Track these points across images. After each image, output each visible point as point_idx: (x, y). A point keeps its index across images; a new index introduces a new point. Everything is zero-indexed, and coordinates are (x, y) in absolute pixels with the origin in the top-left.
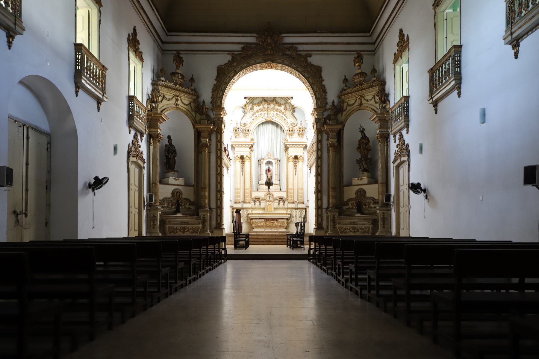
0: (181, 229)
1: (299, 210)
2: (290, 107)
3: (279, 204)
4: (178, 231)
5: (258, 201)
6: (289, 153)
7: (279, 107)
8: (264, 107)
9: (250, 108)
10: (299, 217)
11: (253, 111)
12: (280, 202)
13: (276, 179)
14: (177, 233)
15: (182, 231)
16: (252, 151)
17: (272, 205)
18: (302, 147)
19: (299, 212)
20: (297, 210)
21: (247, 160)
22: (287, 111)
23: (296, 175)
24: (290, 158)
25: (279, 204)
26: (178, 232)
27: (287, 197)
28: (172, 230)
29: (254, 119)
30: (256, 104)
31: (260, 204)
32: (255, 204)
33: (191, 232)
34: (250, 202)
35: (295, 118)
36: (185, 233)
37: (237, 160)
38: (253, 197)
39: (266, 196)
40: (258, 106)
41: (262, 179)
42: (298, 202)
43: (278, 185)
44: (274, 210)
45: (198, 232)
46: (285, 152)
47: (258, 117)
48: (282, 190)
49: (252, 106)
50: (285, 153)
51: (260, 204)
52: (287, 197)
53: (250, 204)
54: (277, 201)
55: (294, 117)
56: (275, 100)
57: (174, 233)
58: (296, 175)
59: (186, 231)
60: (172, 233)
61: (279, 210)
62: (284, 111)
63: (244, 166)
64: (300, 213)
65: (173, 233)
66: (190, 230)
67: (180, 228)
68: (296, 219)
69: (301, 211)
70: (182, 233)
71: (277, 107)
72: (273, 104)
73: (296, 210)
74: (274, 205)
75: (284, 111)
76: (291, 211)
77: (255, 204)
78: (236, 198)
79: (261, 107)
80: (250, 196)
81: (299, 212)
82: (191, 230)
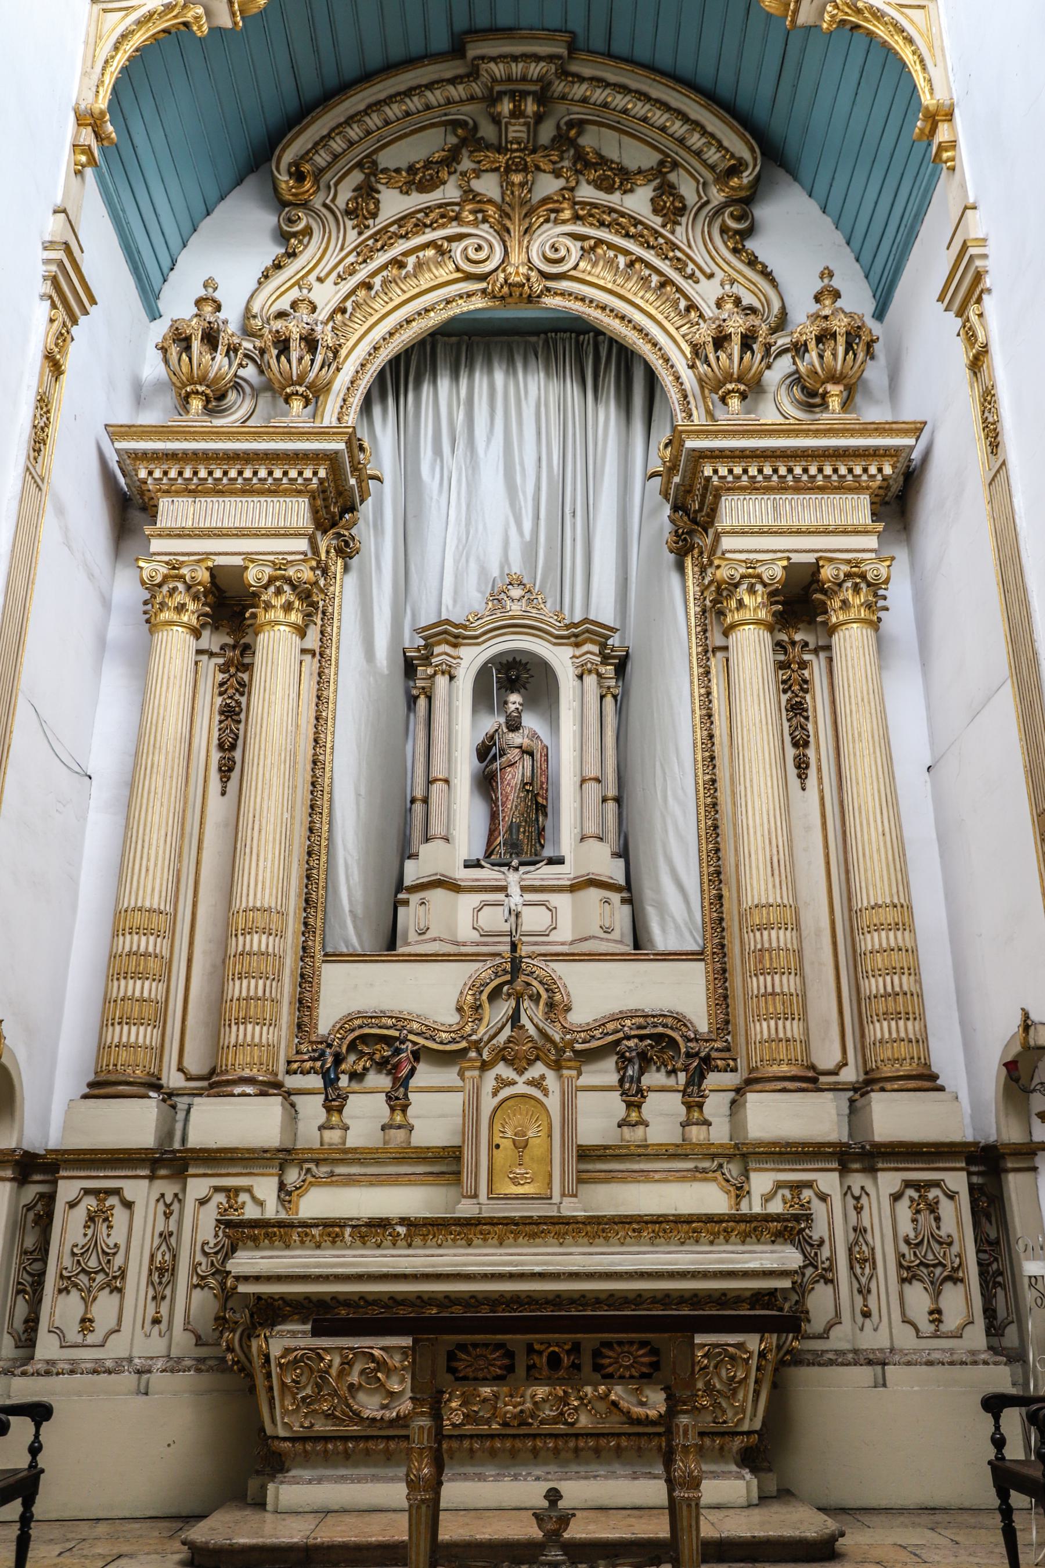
1: (889, 1181)
2: (714, 190)
3: (634, 1100)
5: (382, 1065)
6: (727, 543)
7: (610, 190)
8: (470, 195)
9: (343, 206)
10: (908, 1275)
11: (371, 222)
12: (646, 1080)
13: (591, 828)
16: (346, 550)
17: (553, 1102)
18: (857, 489)
19: (896, 1197)
20: (871, 1170)
21: (271, 615)
22: (684, 220)
23: (802, 776)
24: (742, 592)
25: (634, 1100)
27: (724, 1024)
29: (377, 281)
30: (398, 171)
31: (398, 1102)
32: (335, 1103)
34: (292, 1082)
35: (767, 274)
37: (165, 616)
38: (326, 1020)
39: (477, 1008)
40: (423, 188)
41: (436, 829)
42: (850, 1075)
43: (616, 897)
44: (580, 1181)
46: (681, 568)
47: (419, 265)
48: (662, 939)
49: (367, 192)
50: (675, 578)
51: (398, 1102)
52: (724, 1024)
53: (274, 1105)
54: (606, 1073)
55: (752, 262)
56: (573, 143)
58: (802, 776)
61: (645, 1177)
62: (655, 222)
63: (244, 688)
64: (904, 1210)
68: (864, 1291)
69: (916, 1185)
71: (587, 192)
72: (557, 174)
73: (857, 1181)
74: (568, 1106)
75: (659, 220)
76: (797, 1187)
77: (335, 1103)
78: (116, 1034)
79: (450, 192)
80: (286, 1014)
81: (896, 1197)
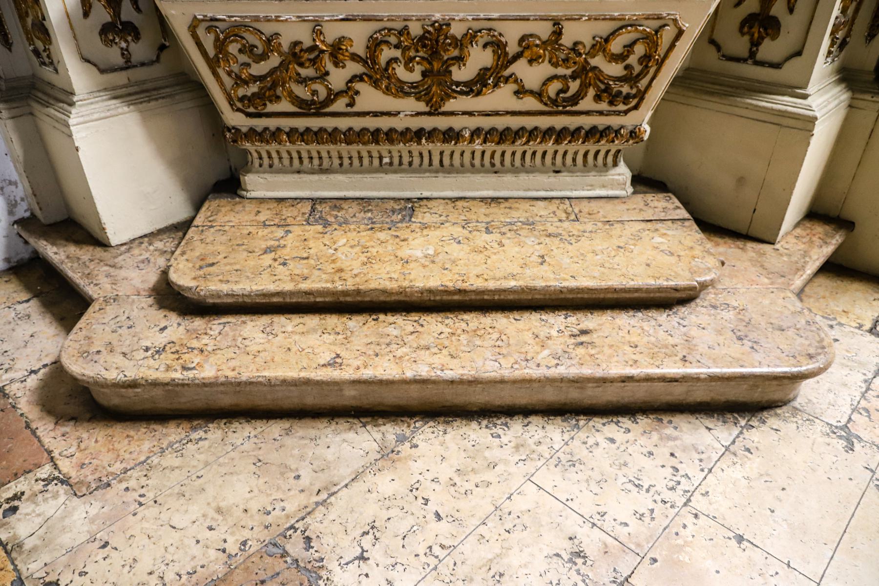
0: (386, 54)
4: (354, 78)
14: (340, 105)
15: (401, 72)
26: (349, 92)
28: (260, 69)
33: (538, 95)
36: (451, 105)
45: (641, 96)
57: (296, 100)
59: (461, 74)
60: (271, 108)
65: (285, 106)
66: (520, 68)
67: (375, 44)
70: (422, 107)
82: (544, 69)
